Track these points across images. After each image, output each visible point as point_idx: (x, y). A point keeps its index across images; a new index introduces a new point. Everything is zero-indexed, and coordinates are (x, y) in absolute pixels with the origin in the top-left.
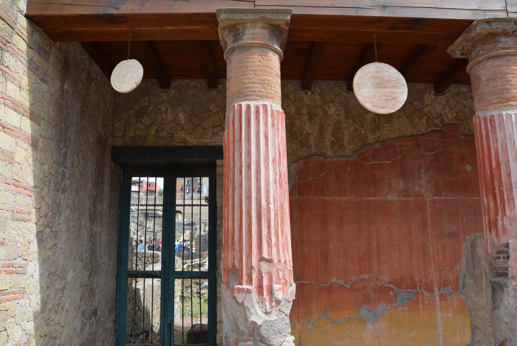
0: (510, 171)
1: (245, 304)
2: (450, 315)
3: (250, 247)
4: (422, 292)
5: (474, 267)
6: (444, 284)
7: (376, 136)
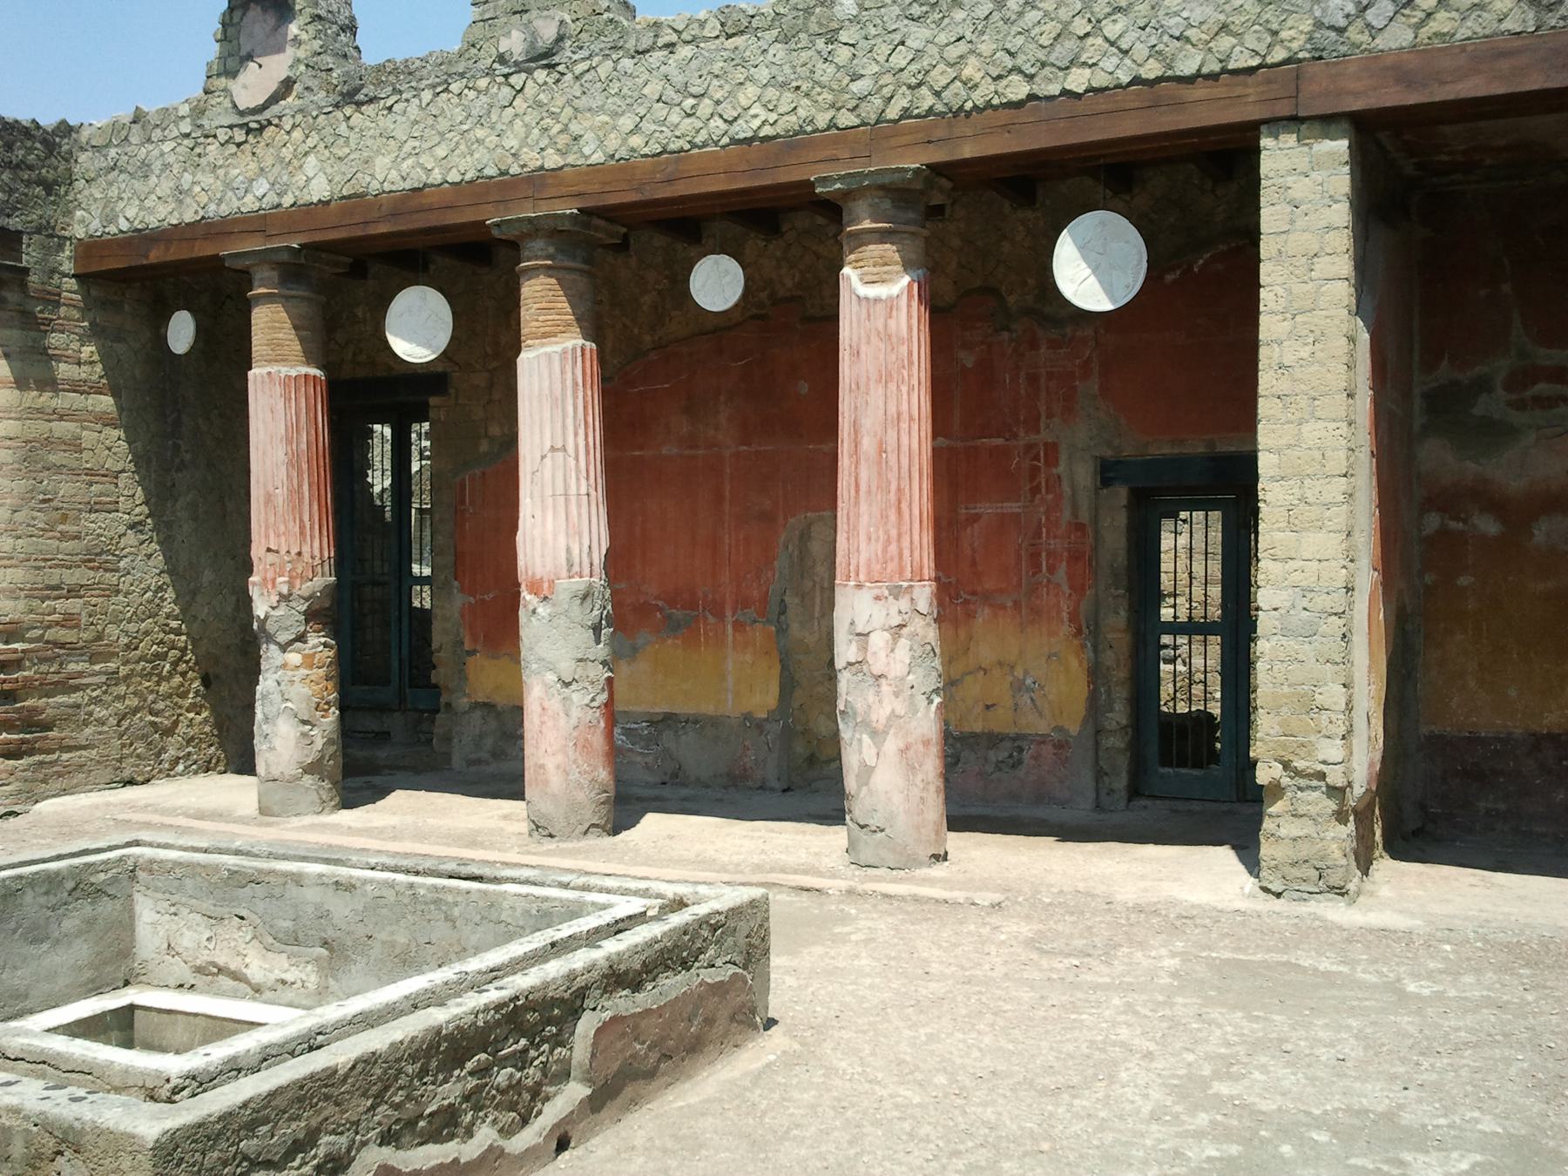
2: (748, 658)
5: (802, 576)
6: (743, 603)
7: (656, 338)
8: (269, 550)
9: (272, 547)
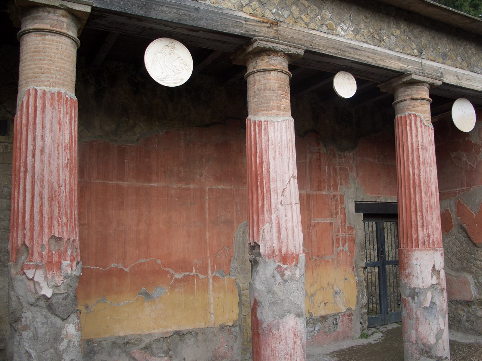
0: (269, 168)
1: (36, 279)
2: (221, 295)
3: (42, 226)
4: (197, 275)
8: (53, 237)
9: (57, 235)
